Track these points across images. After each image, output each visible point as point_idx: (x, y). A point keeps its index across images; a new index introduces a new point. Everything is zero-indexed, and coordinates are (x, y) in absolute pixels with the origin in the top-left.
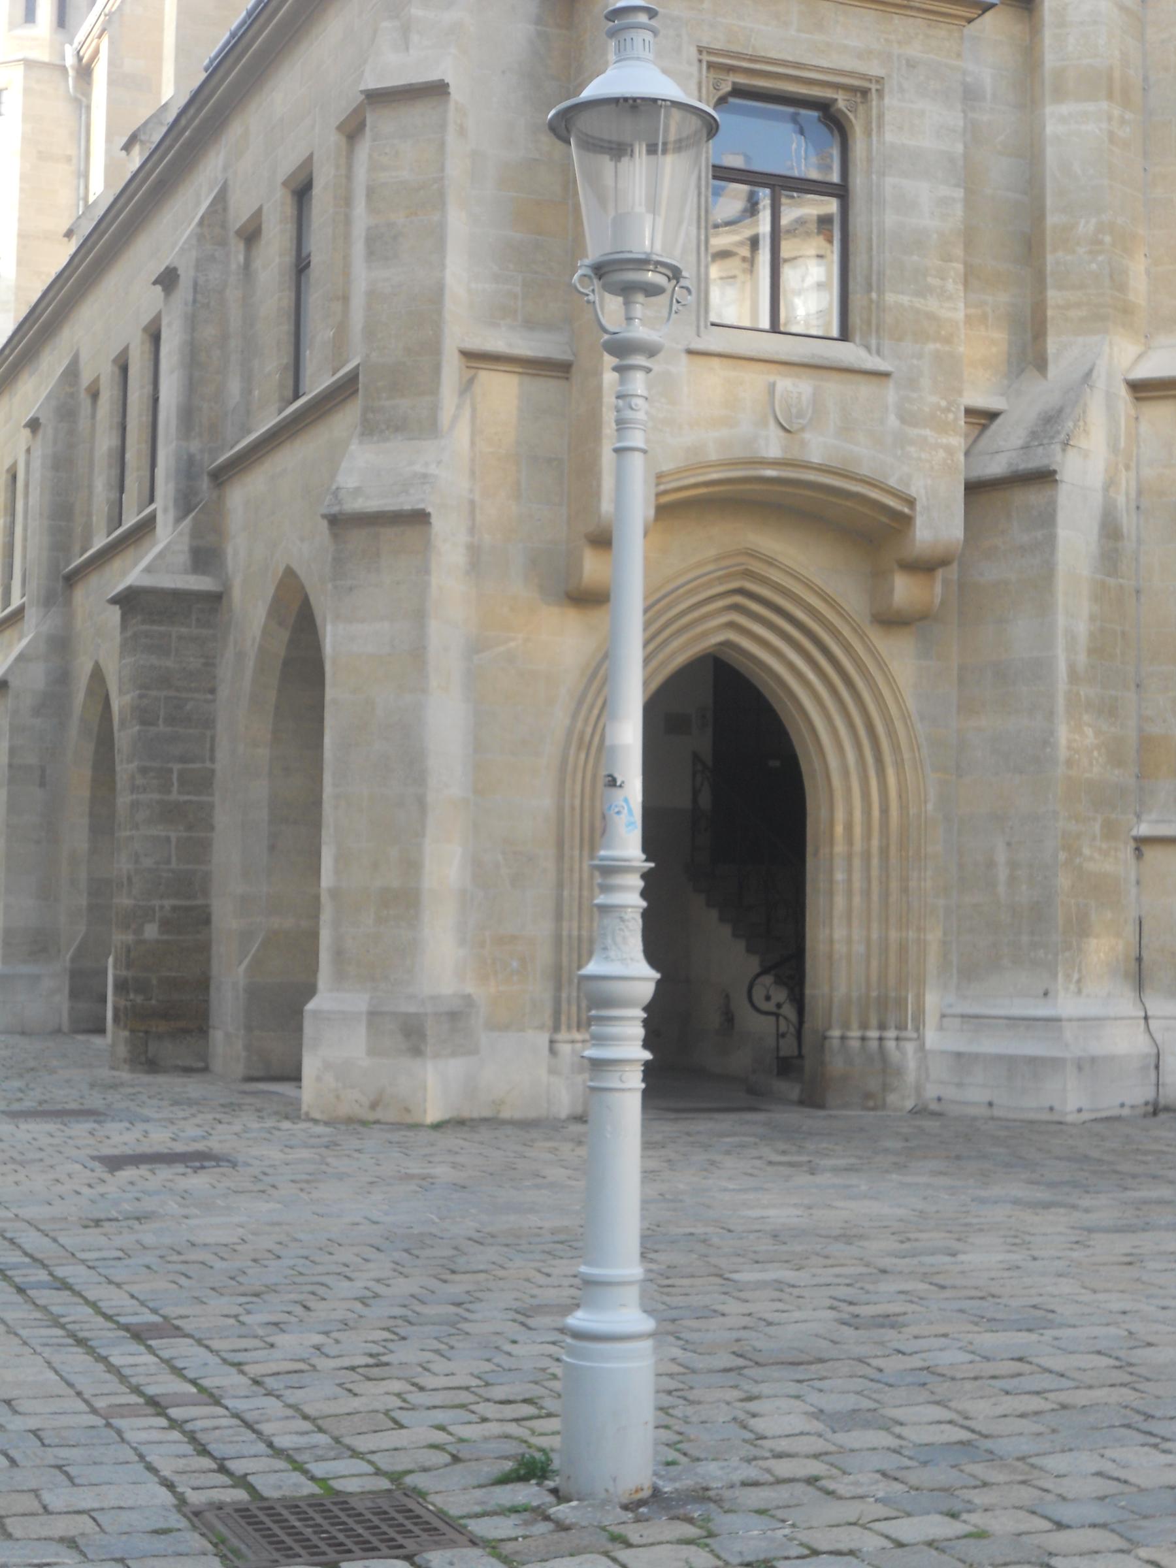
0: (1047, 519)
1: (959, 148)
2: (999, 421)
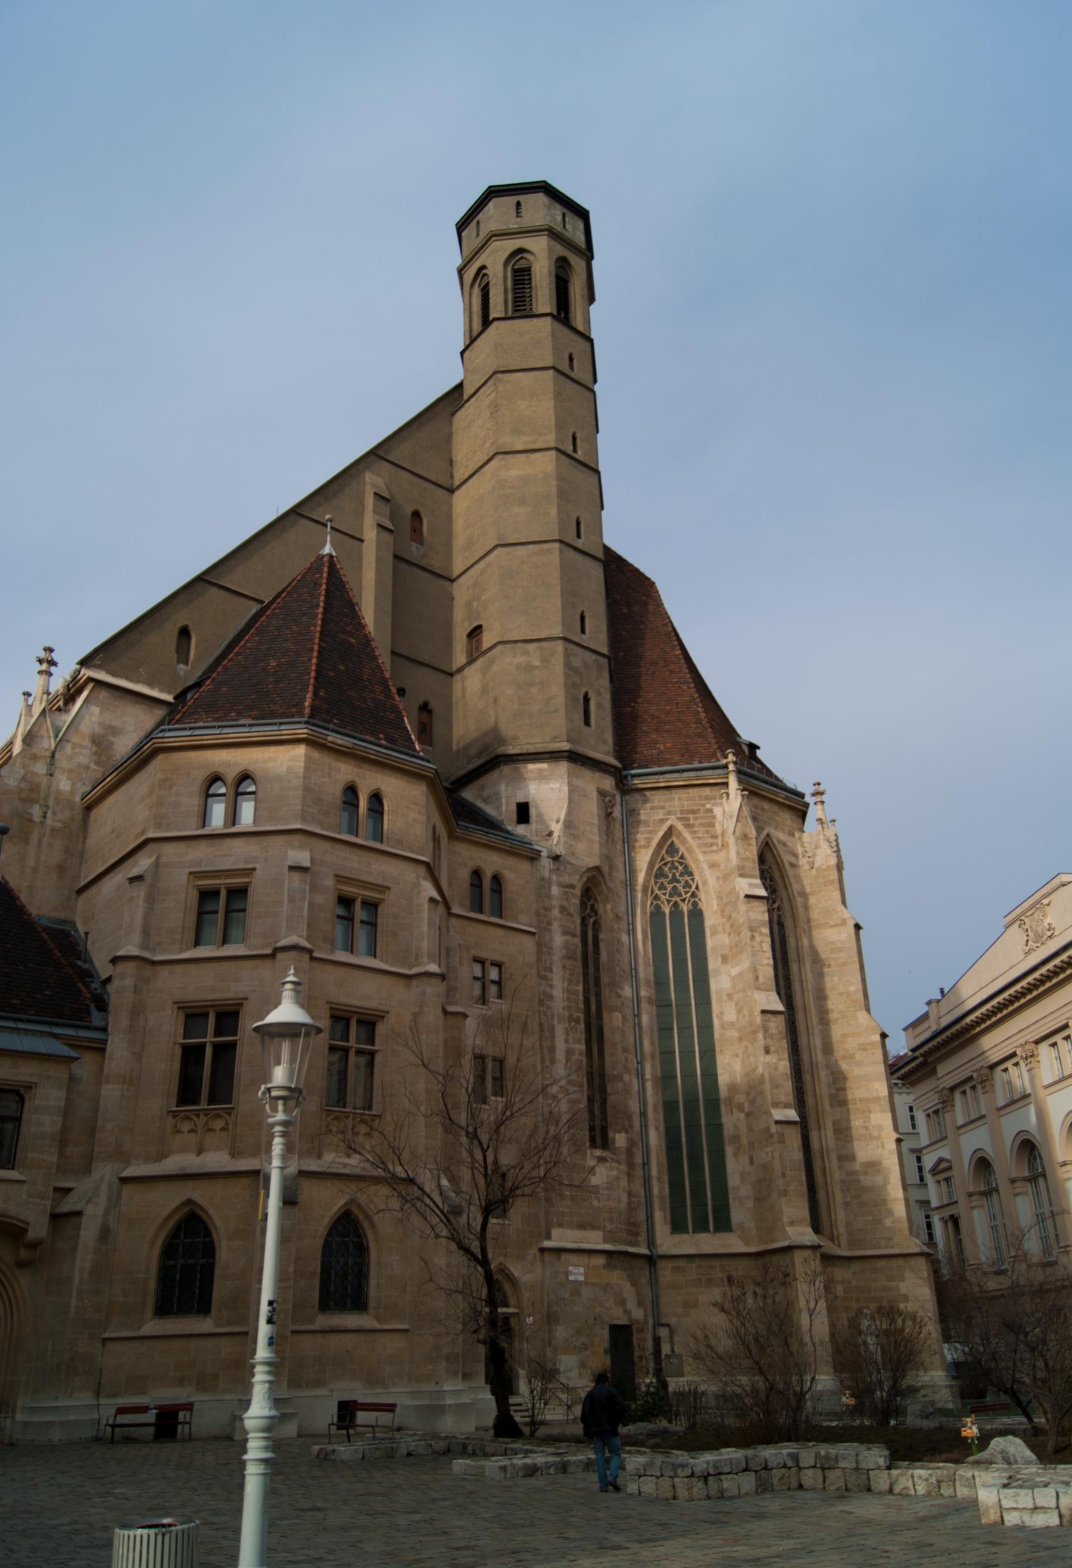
0: (78, 1228)
1: (63, 1104)
2: (73, 1192)
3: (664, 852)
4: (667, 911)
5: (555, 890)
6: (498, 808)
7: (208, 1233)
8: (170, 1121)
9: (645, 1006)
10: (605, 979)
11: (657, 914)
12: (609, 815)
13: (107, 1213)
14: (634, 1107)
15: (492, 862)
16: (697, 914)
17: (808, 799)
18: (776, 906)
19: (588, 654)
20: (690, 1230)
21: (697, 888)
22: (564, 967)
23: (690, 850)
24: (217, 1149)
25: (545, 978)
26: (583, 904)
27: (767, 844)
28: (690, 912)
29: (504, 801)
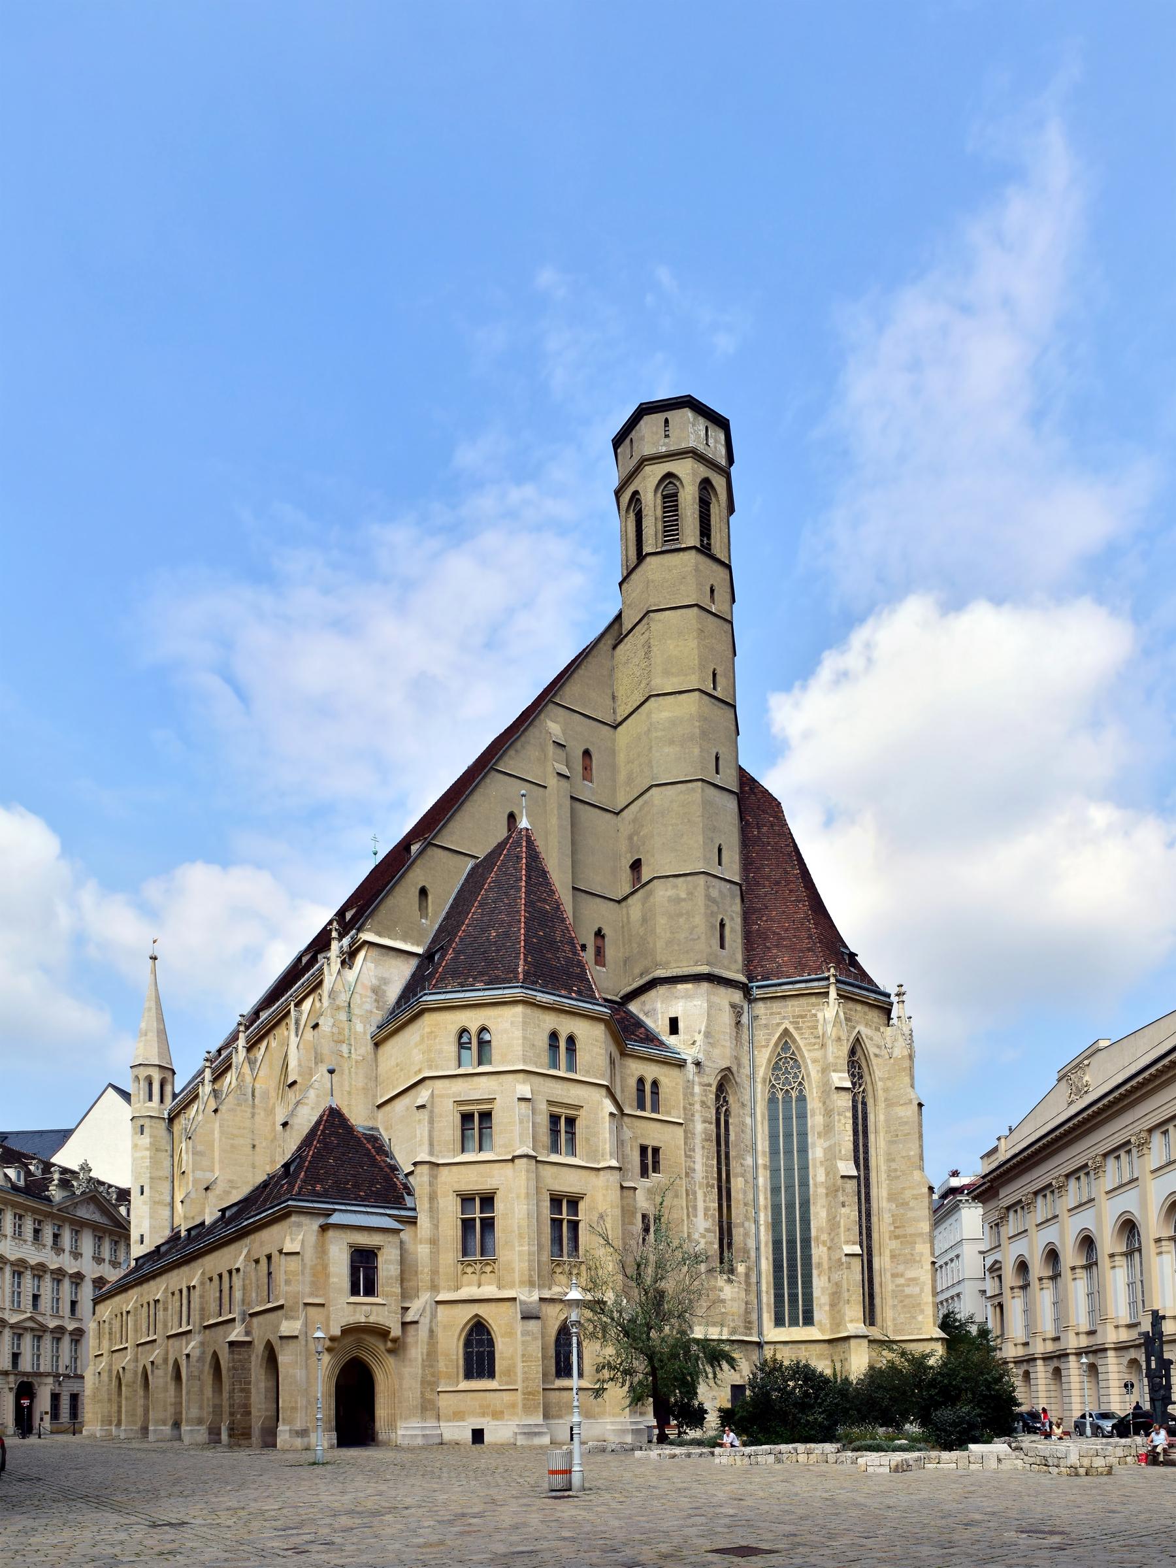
3: (779, 1050)
4: (780, 1097)
5: (697, 1089)
6: (655, 1022)
7: (489, 1333)
8: (460, 1267)
9: (761, 1171)
10: (732, 1153)
11: (772, 1100)
12: (738, 1023)
13: (431, 1322)
14: (752, 1244)
15: (651, 1072)
16: (802, 1099)
17: (894, 999)
18: (861, 1089)
19: (723, 883)
20: (787, 1325)
21: (803, 1078)
22: (703, 1147)
23: (798, 1048)
24: (489, 1284)
25: (690, 1157)
26: (718, 1097)
27: (858, 1039)
28: (797, 1097)
29: (660, 1016)
